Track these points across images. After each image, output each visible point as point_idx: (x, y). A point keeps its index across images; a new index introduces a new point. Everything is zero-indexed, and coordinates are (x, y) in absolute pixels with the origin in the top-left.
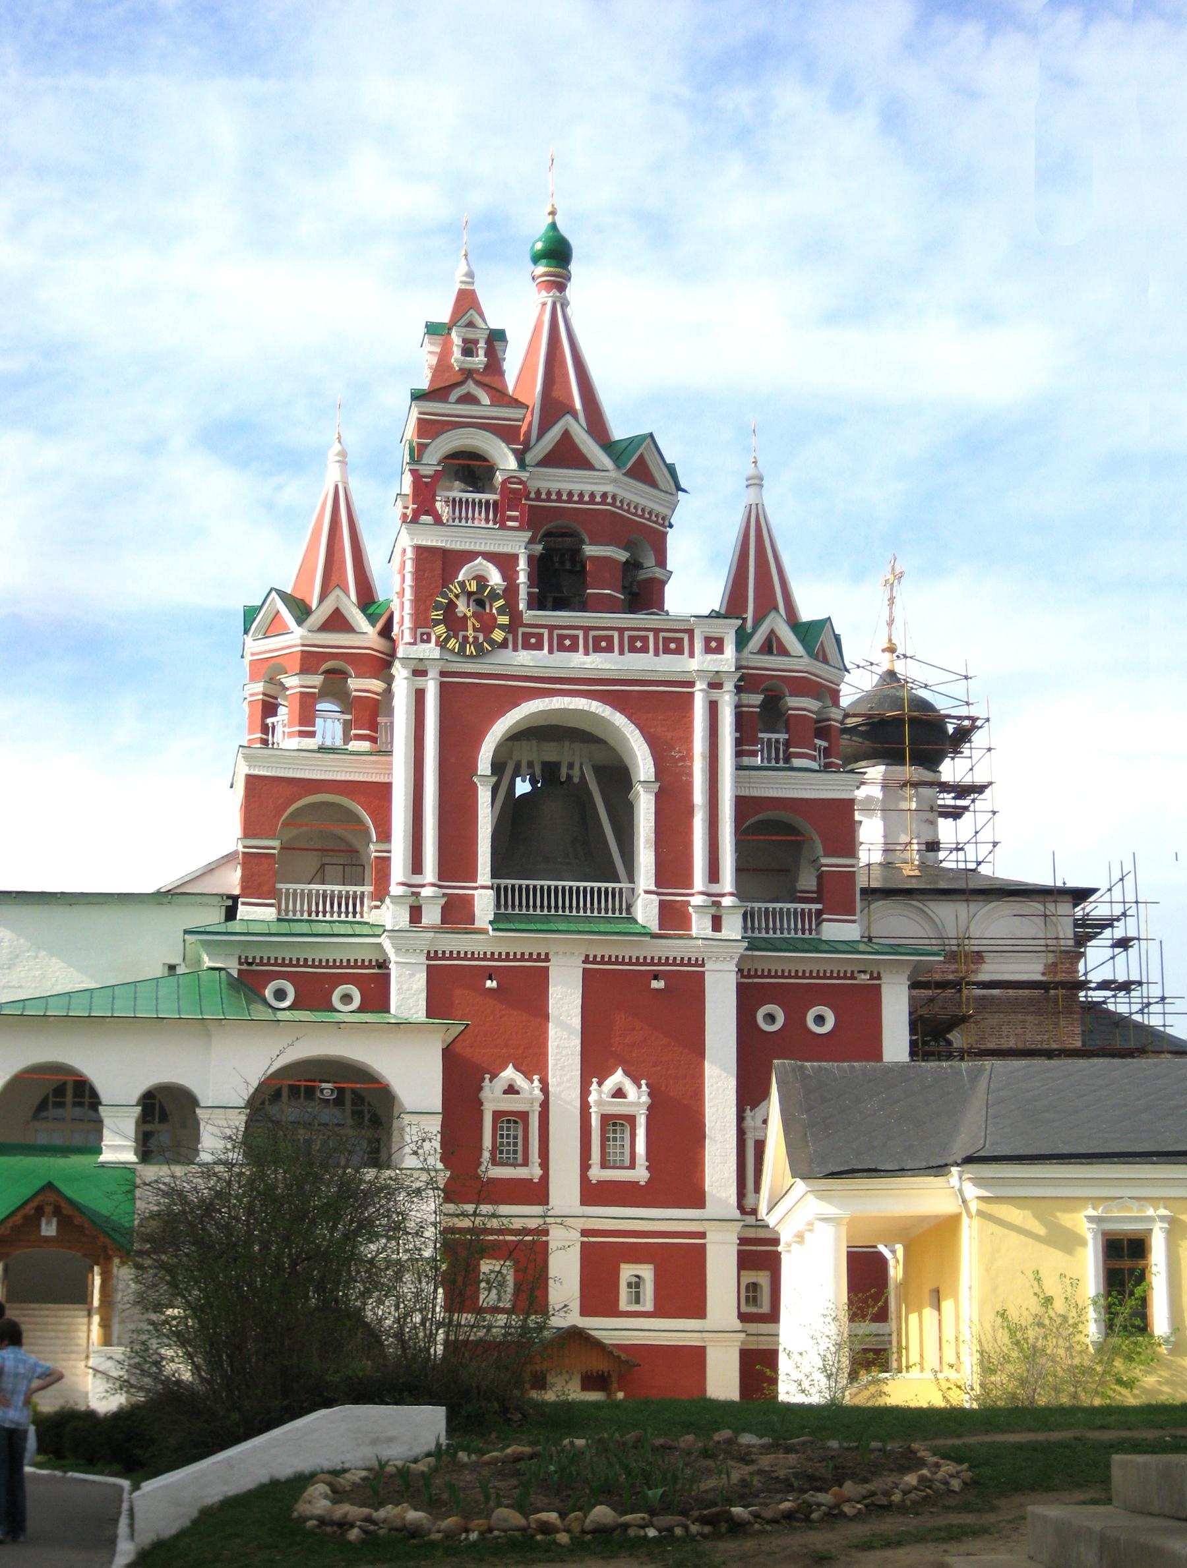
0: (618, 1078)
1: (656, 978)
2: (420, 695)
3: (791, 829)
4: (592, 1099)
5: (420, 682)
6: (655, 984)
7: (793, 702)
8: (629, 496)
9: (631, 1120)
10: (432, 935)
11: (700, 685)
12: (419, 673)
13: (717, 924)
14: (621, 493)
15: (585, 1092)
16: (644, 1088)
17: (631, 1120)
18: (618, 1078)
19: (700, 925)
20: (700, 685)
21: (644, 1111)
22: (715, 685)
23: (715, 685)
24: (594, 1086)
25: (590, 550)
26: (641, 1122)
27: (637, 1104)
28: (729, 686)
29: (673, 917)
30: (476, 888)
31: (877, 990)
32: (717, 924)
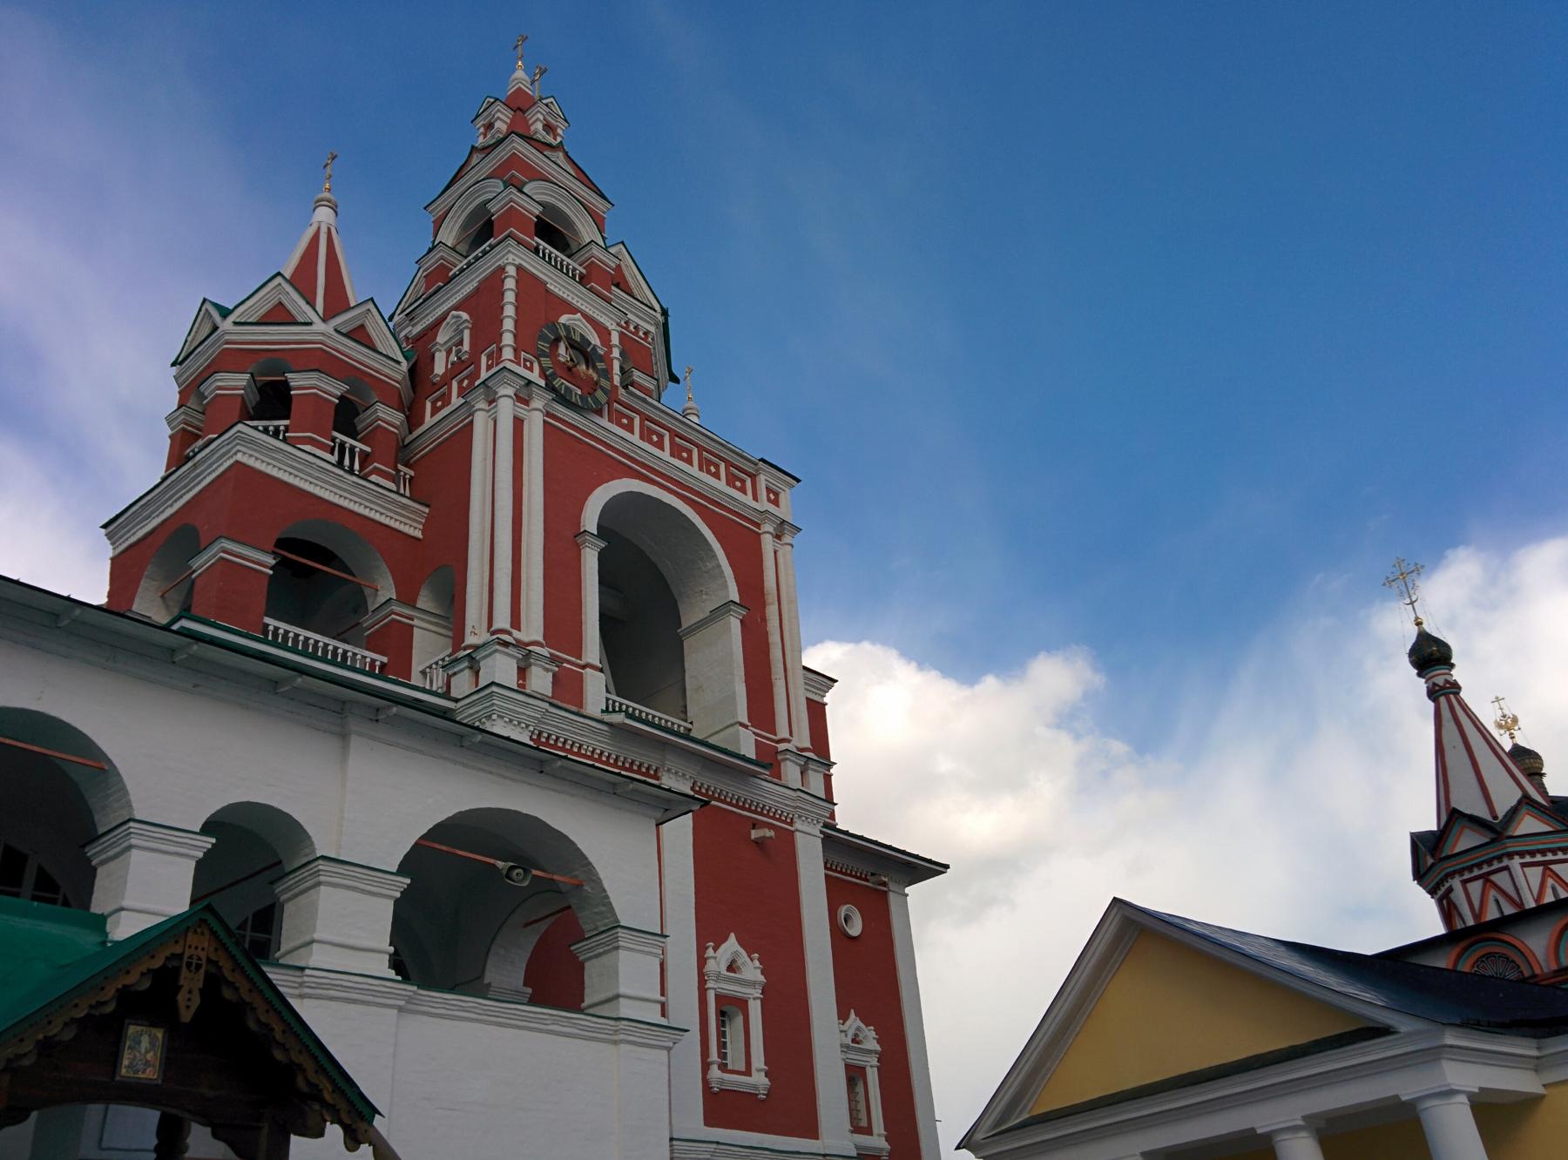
0: (732, 945)
1: (754, 827)
2: (518, 423)
4: (711, 966)
5: (522, 411)
9: (742, 1004)
10: (546, 705)
12: (522, 399)
15: (702, 962)
16: (757, 963)
17: (742, 1004)
18: (732, 945)
21: (757, 993)
24: (710, 952)
26: (755, 1009)
27: (753, 984)
30: (584, 667)
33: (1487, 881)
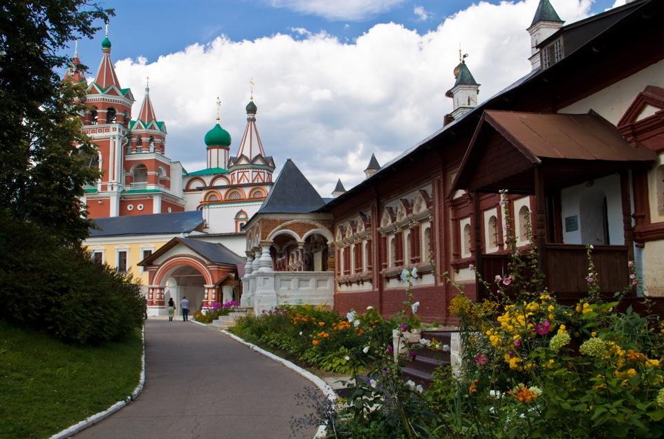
3: (144, 166)
6: (100, 202)
7: (142, 139)
8: (108, 98)
11: (111, 138)
13: (112, 189)
14: (105, 98)
19: (109, 189)
20: (111, 138)
22: (114, 138)
23: (114, 138)
25: (98, 111)
28: (117, 138)
29: (104, 188)
31: (152, 200)
32: (112, 189)
33: (258, 174)
